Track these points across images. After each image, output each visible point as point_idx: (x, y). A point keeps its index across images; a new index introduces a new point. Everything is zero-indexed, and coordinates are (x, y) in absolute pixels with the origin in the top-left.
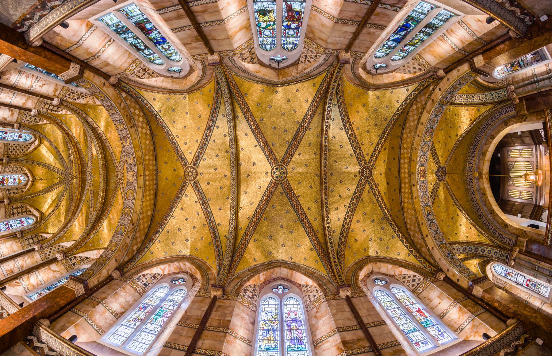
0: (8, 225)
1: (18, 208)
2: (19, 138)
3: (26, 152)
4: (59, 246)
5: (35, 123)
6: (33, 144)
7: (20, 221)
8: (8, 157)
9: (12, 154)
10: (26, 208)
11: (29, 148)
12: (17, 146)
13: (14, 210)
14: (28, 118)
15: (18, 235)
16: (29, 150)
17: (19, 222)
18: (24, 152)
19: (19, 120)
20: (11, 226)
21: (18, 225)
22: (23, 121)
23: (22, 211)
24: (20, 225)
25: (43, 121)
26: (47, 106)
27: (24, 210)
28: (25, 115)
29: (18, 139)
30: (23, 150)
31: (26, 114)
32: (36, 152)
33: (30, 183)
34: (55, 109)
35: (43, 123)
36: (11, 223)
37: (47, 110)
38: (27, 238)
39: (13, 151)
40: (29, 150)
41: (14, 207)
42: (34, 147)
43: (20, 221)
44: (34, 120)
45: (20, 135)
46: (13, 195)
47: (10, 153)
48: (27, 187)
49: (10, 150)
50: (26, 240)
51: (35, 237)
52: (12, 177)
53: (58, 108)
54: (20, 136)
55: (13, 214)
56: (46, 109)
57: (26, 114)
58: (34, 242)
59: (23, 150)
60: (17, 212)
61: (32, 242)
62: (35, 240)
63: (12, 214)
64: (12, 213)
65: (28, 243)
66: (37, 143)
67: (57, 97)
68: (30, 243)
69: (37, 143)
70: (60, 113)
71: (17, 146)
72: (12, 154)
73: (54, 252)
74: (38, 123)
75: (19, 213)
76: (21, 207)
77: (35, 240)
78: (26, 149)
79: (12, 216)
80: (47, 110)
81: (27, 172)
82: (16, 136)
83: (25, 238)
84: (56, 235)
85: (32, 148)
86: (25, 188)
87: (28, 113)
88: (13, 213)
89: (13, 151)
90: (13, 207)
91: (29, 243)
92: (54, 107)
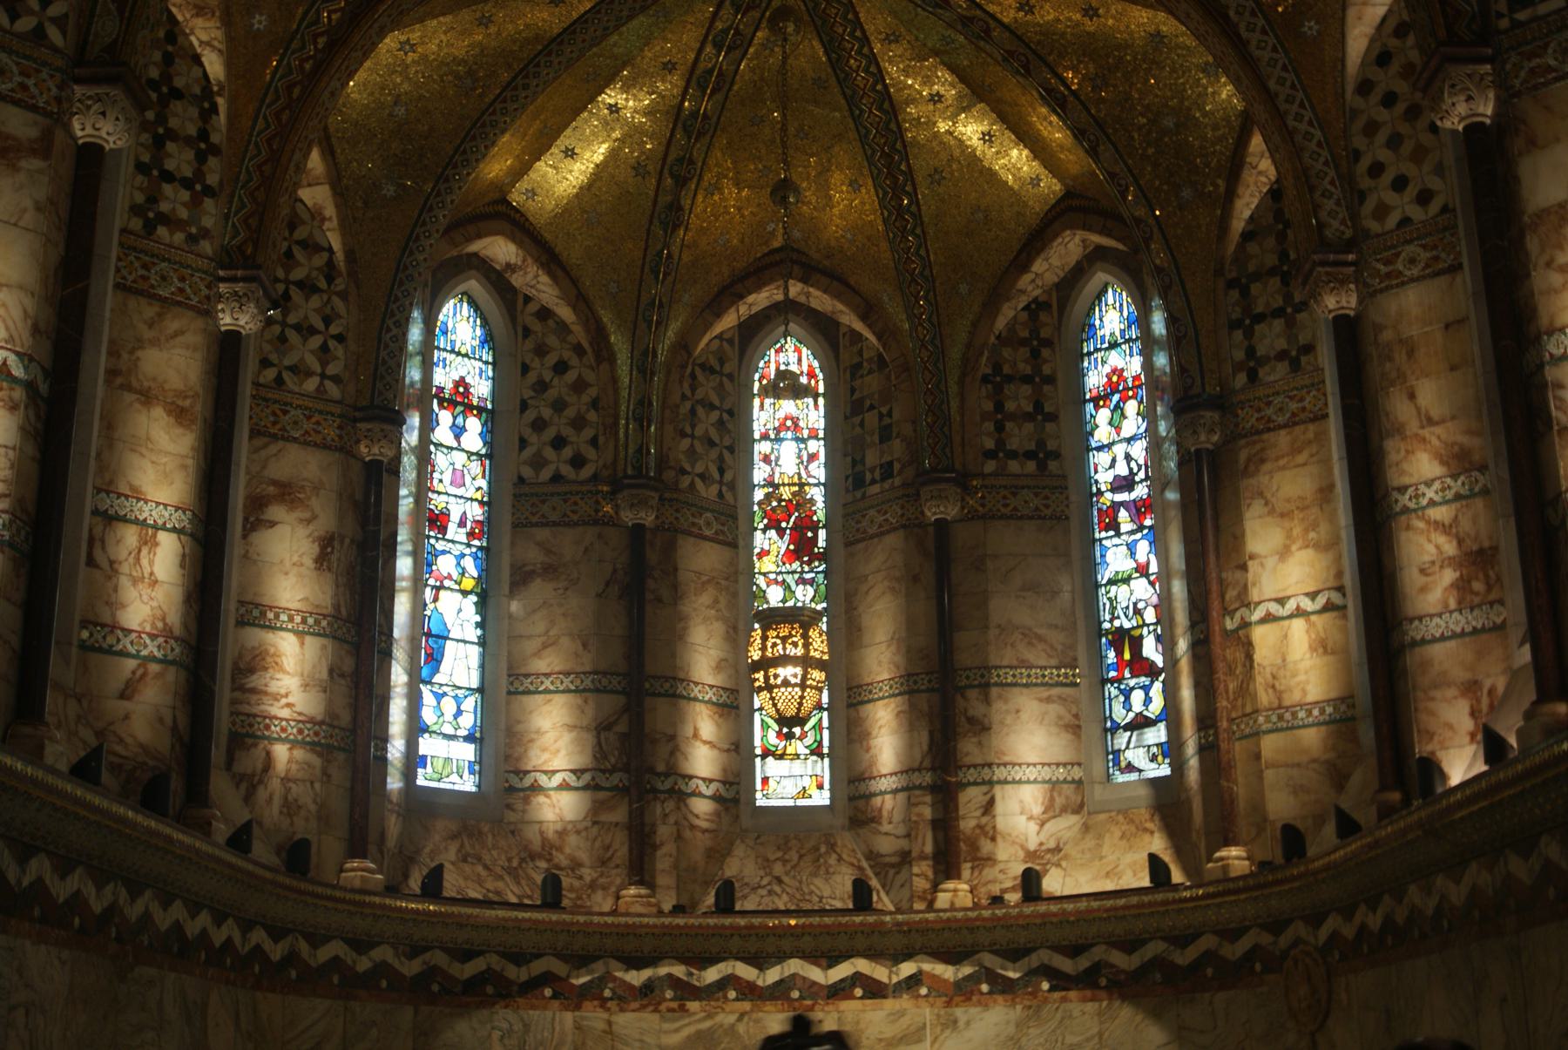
0: (1116, 506)
1: (999, 407)
2: (469, 408)
3: (579, 334)
4: (1365, 87)
5: (340, 284)
6: (517, 280)
8: (617, 486)
9: (591, 453)
10: (1008, 339)
11: (545, 314)
12: (530, 415)
13: (1013, 444)
14: (304, 351)
15: (1209, 439)
16: (565, 313)
18: (579, 350)
19: (331, 432)
20: (1125, 483)
22: (333, 390)
23: (1027, 379)
24: (1131, 407)
25: (317, 215)
26: (174, 199)
27: (1017, 360)
28: (279, 381)
30: (561, 368)
31: (270, 374)
32: (573, 254)
33: (820, 300)
34: (183, 118)
35: (330, 211)
37: (209, 191)
38: (1238, 367)
39: (568, 452)
40: (565, 313)
41: (989, 444)
42: (533, 269)
44: (315, 301)
45: (449, 403)
46: (897, 447)
47: (586, 472)
48: (850, 320)
49: (566, 470)
50: (1253, 377)
51: (1245, 292)
53: (177, 94)
54: (459, 399)
55: (1042, 455)
56: (195, 202)
57: (270, 374)
58: (1279, 313)
59: (561, 368)
60: (1029, 417)
61: (1278, 324)
62: (1266, 295)
63: (1042, 466)
64: (1031, 466)
65: (1282, 368)
66: (501, 249)
67: (58, 118)
68: (1282, 344)
69: (501, 249)
70: (214, 65)
71: (530, 415)
72: (591, 453)
73: (1407, 148)
74: (340, 256)
75: (1038, 406)
76: (998, 380)
77: (1266, 295)
78: (552, 341)
79: (1053, 465)
80: (209, 191)
81: (728, 321)
82: (458, 431)
83: (1241, 379)
84: (1271, 97)
85: (542, 287)
86: (856, 337)
87: (265, 363)
88: (1030, 455)
89: (568, 452)
90: (990, 455)
91: (1282, 355)
92: (172, 135)
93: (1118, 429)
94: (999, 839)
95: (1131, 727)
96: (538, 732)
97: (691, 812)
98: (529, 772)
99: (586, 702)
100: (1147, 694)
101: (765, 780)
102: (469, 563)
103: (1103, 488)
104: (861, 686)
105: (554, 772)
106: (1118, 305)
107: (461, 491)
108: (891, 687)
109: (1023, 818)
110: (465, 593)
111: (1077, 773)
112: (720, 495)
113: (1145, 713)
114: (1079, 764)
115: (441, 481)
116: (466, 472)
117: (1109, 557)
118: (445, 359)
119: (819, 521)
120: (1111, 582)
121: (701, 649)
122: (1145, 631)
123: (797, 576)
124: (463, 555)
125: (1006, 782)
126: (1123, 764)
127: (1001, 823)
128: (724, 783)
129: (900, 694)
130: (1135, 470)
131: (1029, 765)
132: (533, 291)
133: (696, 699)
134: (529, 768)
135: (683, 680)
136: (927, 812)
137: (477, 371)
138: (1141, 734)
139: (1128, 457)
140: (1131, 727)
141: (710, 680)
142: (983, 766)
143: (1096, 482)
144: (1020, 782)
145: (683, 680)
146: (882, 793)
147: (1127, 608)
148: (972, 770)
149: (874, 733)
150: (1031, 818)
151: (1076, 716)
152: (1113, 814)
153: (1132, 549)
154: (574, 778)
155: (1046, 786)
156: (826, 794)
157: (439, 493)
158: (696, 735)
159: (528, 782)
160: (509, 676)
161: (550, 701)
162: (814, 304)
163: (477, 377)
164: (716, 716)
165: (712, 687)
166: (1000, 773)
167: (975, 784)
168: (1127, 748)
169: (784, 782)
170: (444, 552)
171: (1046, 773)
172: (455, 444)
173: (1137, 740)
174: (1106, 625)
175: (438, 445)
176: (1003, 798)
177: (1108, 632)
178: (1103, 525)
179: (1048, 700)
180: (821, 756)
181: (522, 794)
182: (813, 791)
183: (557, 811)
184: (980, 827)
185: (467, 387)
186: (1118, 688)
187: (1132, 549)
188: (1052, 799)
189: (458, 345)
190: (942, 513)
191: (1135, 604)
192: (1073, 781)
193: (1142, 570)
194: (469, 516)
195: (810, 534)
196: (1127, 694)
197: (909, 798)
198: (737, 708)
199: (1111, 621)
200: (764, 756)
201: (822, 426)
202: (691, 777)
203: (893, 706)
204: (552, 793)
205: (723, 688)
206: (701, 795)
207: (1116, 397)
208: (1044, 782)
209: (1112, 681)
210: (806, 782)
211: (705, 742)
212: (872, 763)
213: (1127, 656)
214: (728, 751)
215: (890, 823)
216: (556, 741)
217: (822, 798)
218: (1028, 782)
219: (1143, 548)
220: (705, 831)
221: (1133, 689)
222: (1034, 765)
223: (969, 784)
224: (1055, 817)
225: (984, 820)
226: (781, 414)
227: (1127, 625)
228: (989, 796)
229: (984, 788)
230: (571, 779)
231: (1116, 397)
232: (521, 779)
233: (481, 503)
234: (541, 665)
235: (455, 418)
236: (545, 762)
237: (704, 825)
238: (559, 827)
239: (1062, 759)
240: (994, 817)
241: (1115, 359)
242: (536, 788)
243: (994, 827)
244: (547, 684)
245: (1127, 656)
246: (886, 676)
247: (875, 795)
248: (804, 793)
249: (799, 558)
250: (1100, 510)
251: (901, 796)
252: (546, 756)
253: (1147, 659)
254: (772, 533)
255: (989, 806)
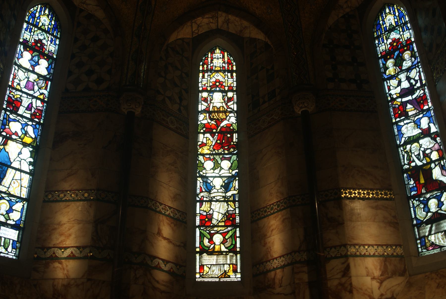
0: (404, 104)
7: (387, 55)
16: (100, 14)
17: (390, 63)
20: (410, 91)
21: (406, 64)
24: (407, 55)
29: (48, 57)
36: (395, 92)
40: (100, 14)
43: (387, 55)
52: (205, 95)
86: (253, 41)
93: (400, 66)
94: (355, 292)
95: (430, 221)
96: (60, 224)
97: (154, 279)
98: (50, 248)
99: (90, 206)
100: (439, 200)
101: (202, 267)
102: (30, 130)
103: (395, 96)
104: (260, 210)
105: (66, 248)
106: (392, 11)
107: (31, 92)
108: (278, 207)
109: (369, 279)
110: (25, 145)
111: (399, 251)
112: (179, 110)
113: (439, 211)
114: (400, 246)
115: (19, 84)
116: (35, 84)
117: (404, 130)
118: (31, 29)
119: (234, 129)
120: (406, 143)
121: (165, 185)
122: (433, 165)
123: (221, 156)
124: (27, 125)
125: (355, 256)
126: (428, 244)
127: (354, 281)
128: (176, 264)
129: (284, 209)
130: (414, 83)
131: (369, 246)
132: (85, 6)
133: (160, 212)
134: (51, 245)
135: (153, 200)
136: (305, 277)
137: (50, 39)
138: (439, 224)
139: (408, 79)
140: (430, 221)
141: (170, 204)
142: (340, 246)
143: (390, 95)
144: (365, 256)
145: (153, 200)
146: (274, 269)
147: (419, 154)
148: (333, 249)
149: (268, 235)
150: (373, 278)
151: (395, 217)
152: (427, 274)
153: (417, 124)
154: (78, 252)
155: (381, 258)
156: (239, 275)
157: (17, 90)
158: (159, 233)
159: (49, 254)
160: (46, 192)
161: (69, 206)
162: (232, 30)
163: (49, 42)
164: (172, 225)
165: (170, 208)
166: (353, 250)
167: (336, 257)
168: (430, 234)
169: (214, 268)
170: (14, 120)
171: (380, 250)
172: (31, 69)
173: (436, 229)
174: (407, 167)
175: (20, 67)
176: (355, 265)
177: (407, 170)
178: (397, 115)
179: (377, 208)
180: (236, 253)
181: (44, 262)
182: (231, 274)
183: (65, 272)
184: (341, 284)
185: (43, 45)
186: (419, 200)
187: (417, 124)
188: (385, 267)
189: (40, 24)
190: (305, 107)
191: (424, 152)
192: (397, 256)
193: (426, 133)
194: (34, 105)
195: (229, 136)
196: (426, 204)
197: (293, 269)
198: (186, 223)
199: (409, 164)
200: (201, 253)
201: (235, 85)
202: (155, 257)
203: (280, 216)
204: (63, 261)
205: (177, 210)
206: (160, 269)
207: (396, 53)
208: (380, 256)
209: (414, 197)
210: (226, 268)
211: (165, 238)
212: (268, 251)
213: (422, 181)
214: (179, 246)
215: (281, 287)
216: (69, 229)
217: (235, 277)
218: (369, 256)
219: (424, 123)
220: (162, 292)
221: (429, 199)
222: (373, 246)
223: (332, 258)
224: (389, 278)
225: (343, 280)
226: (214, 80)
227: (419, 163)
228: (345, 265)
229: (342, 260)
230: (77, 253)
231: (396, 53)
232: (45, 252)
233: (43, 101)
234: (66, 186)
235: (33, 57)
236: (62, 242)
237: (162, 288)
238: (65, 282)
239: (390, 242)
240: (350, 277)
241: (394, 35)
242: (55, 258)
243: (351, 284)
244: (68, 197)
245: (422, 181)
246: (275, 200)
247: (270, 271)
248: (225, 274)
249: (223, 147)
250: (394, 108)
251: (287, 269)
252: (62, 238)
253: (436, 180)
254: (208, 135)
255: (346, 271)
